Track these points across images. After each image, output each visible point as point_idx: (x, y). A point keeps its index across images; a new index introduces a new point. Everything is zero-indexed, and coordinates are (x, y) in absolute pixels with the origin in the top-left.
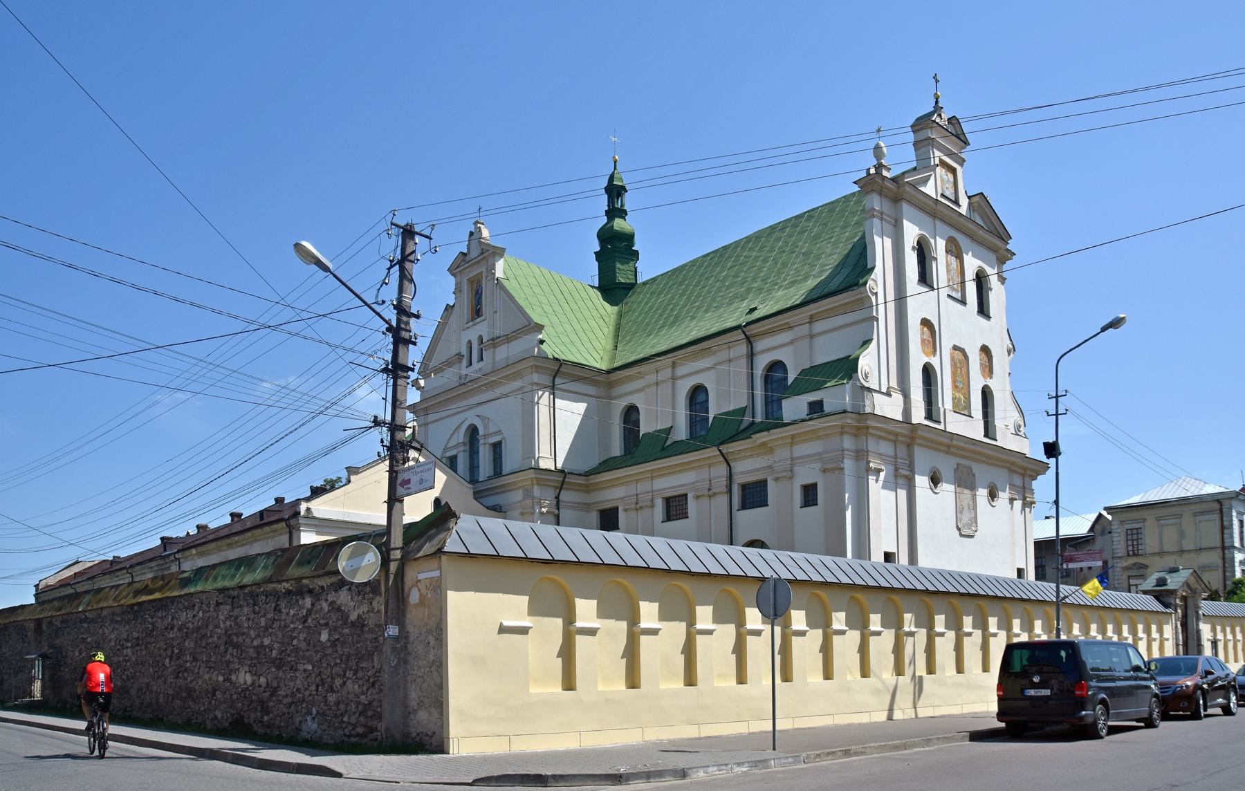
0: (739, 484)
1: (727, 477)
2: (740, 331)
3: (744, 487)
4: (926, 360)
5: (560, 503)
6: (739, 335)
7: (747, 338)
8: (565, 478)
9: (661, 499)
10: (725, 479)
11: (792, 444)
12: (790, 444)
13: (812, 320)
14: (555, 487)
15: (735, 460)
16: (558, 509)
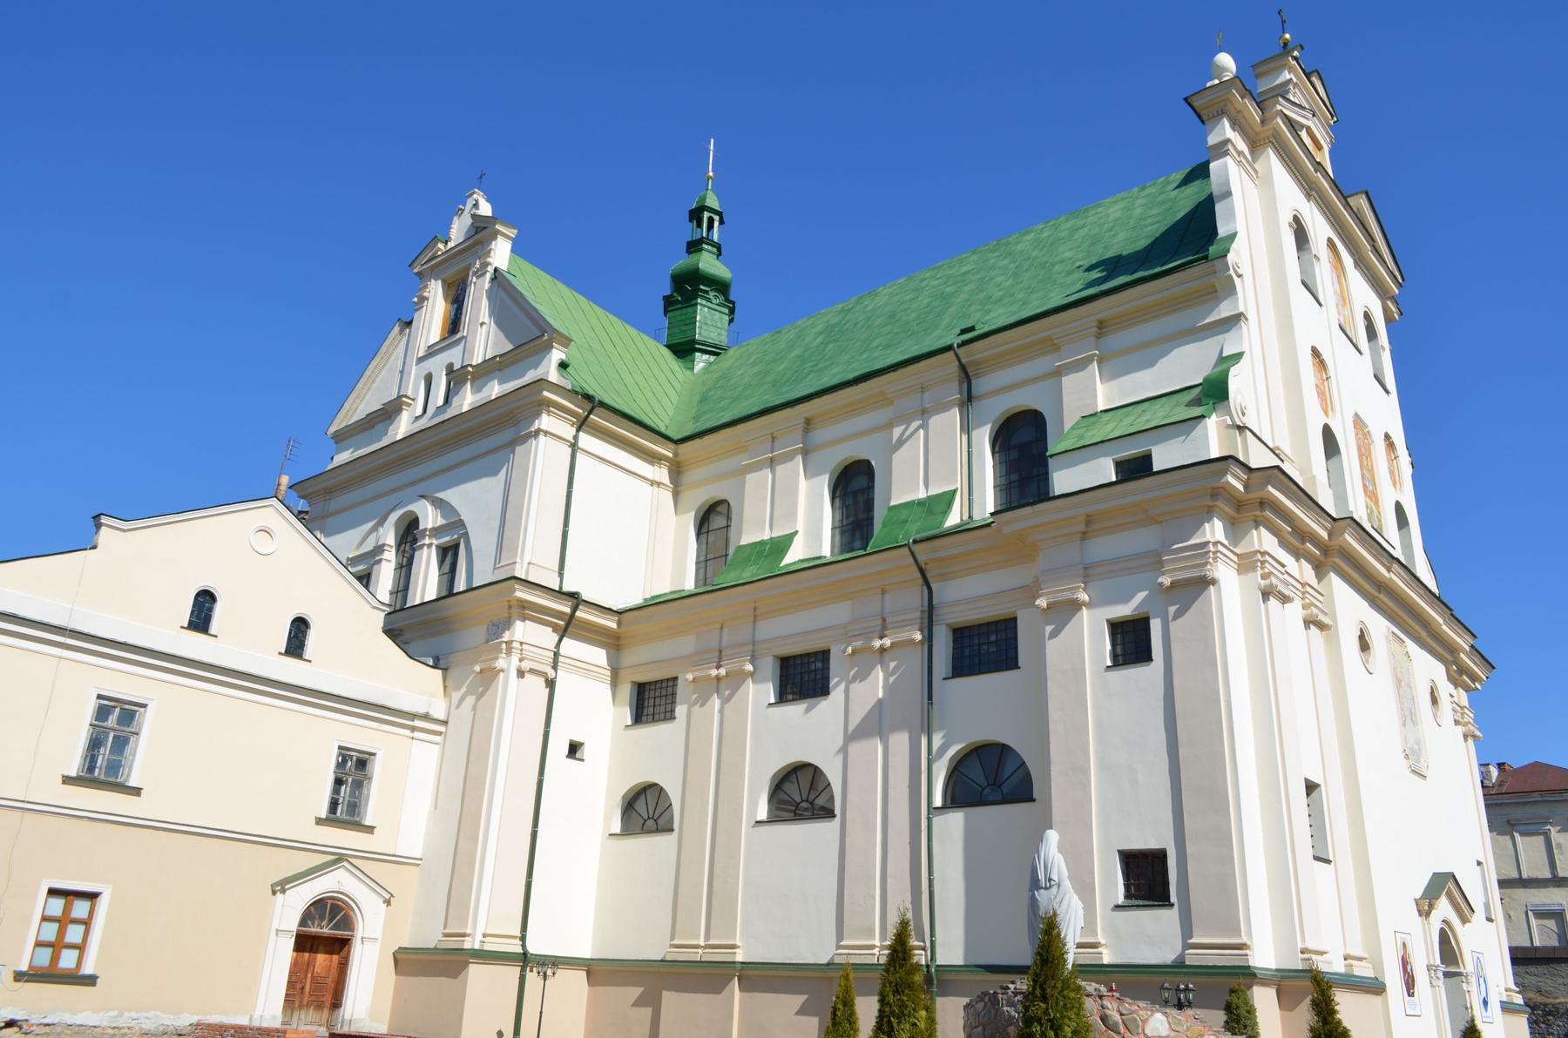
0: (947, 625)
1: (922, 612)
2: (950, 354)
3: (961, 635)
4: (1324, 420)
5: (561, 659)
6: (948, 362)
7: (963, 367)
8: (575, 609)
9: (771, 658)
10: (918, 614)
11: (1084, 536)
12: (1080, 535)
13: (1102, 327)
14: (555, 628)
15: (944, 577)
16: (555, 667)
